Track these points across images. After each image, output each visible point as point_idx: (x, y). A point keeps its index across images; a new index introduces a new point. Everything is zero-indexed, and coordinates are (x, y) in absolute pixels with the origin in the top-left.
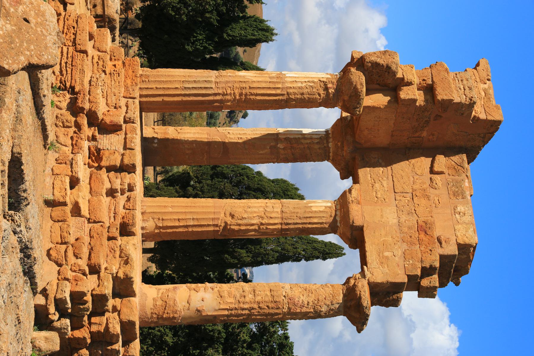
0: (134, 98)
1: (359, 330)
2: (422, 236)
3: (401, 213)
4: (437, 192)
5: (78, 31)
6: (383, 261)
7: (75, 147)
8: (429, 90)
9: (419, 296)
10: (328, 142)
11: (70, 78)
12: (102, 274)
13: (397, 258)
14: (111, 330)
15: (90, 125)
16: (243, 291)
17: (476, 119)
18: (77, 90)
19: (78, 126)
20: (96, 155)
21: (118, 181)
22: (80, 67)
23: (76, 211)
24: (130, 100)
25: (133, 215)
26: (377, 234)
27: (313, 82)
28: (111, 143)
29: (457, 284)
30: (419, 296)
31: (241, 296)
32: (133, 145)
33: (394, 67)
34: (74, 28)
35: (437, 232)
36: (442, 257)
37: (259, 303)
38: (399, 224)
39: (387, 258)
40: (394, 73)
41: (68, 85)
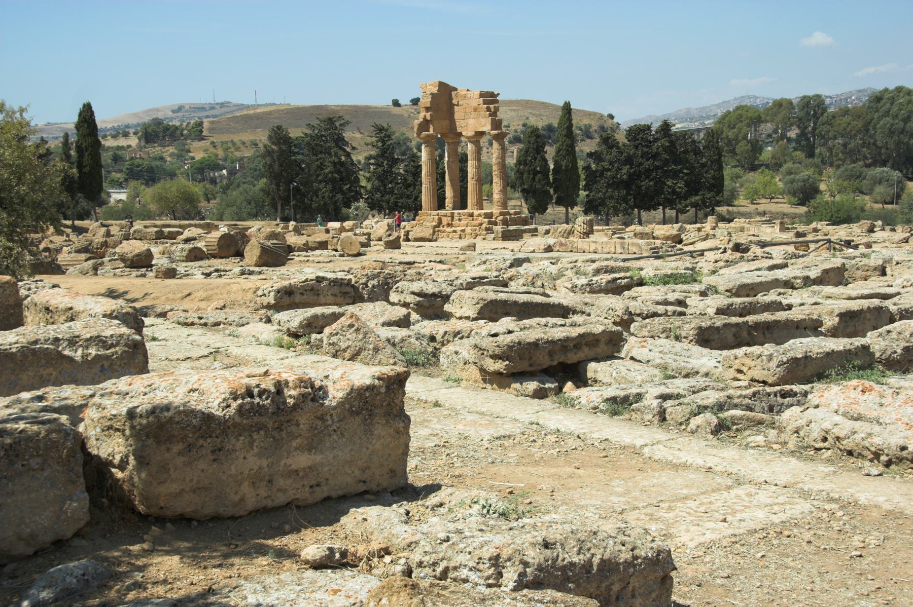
6: (485, 125)
7: (444, 232)
20: (449, 225)
23: (463, 231)
28: (445, 221)
29: (498, 94)
36: (484, 104)
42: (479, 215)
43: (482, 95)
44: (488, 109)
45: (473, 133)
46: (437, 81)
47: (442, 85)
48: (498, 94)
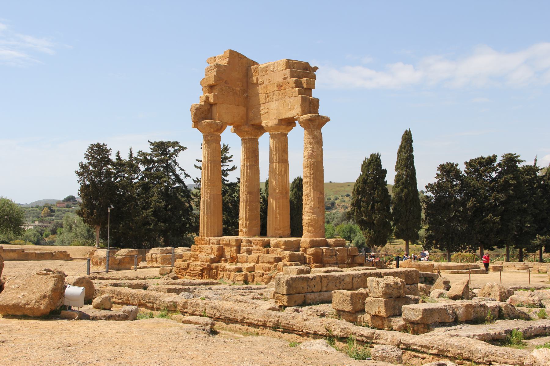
0: (210, 240)
1: (328, 120)
2: (282, 88)
4: (265, 81)
6: (292, 108)
8: (211, 88)
9: (314, 88)
10: (246, 139)
12: (281, 256)
14: (312, 252)
15: (219, 262)
17: (229, 63)
18: (201, 268)
19: (217, 268)
20: (233, 260)
21: (244, 249)
23: (251, 270)
24: (211, 242)
28: (229, 252)
30: (314, 88)
33: (197, 106)
35: (281, 80)
36: (292, 77)
37: (311, 174)
39: (291, 106)
40: (201, 105)
41: (200, 273)
42: (277, 246)
43: (289, 64)
44: (298, 84)
45: (276, 122)
46: (227, 48)
47: (234, 56)
48: (316, 68)
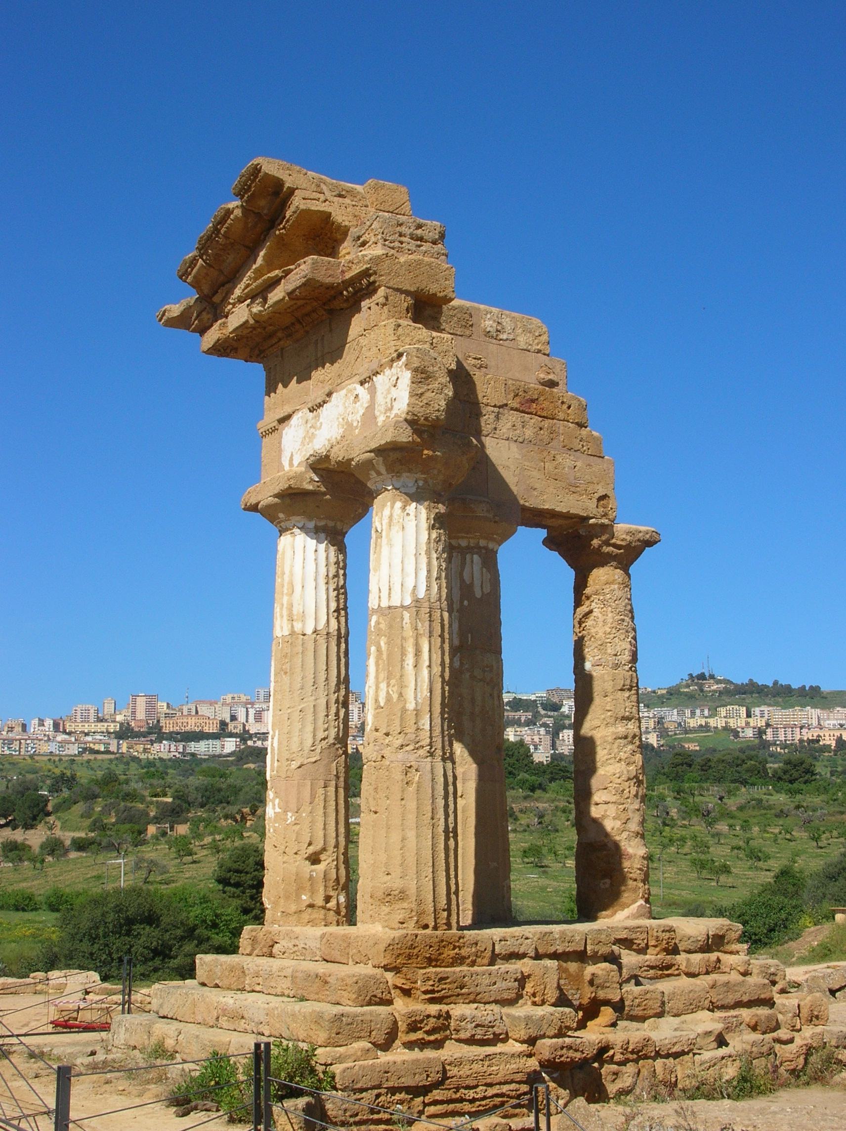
3: (498, 432)
5: (390, 1084)
11: (513, 1086)
13: (579, 464)
16: (626, 737)
22: (476, 1067)
25: (663, 931)
26: (537, 486)
27: (437, 541)
31: (632, 743)
32: (577, 938)
34: (378, 1096)
38: (521, 442)
